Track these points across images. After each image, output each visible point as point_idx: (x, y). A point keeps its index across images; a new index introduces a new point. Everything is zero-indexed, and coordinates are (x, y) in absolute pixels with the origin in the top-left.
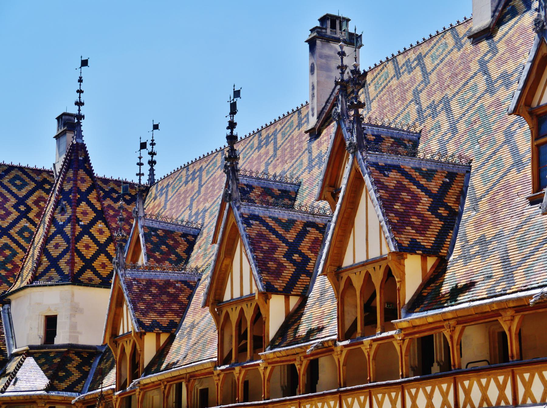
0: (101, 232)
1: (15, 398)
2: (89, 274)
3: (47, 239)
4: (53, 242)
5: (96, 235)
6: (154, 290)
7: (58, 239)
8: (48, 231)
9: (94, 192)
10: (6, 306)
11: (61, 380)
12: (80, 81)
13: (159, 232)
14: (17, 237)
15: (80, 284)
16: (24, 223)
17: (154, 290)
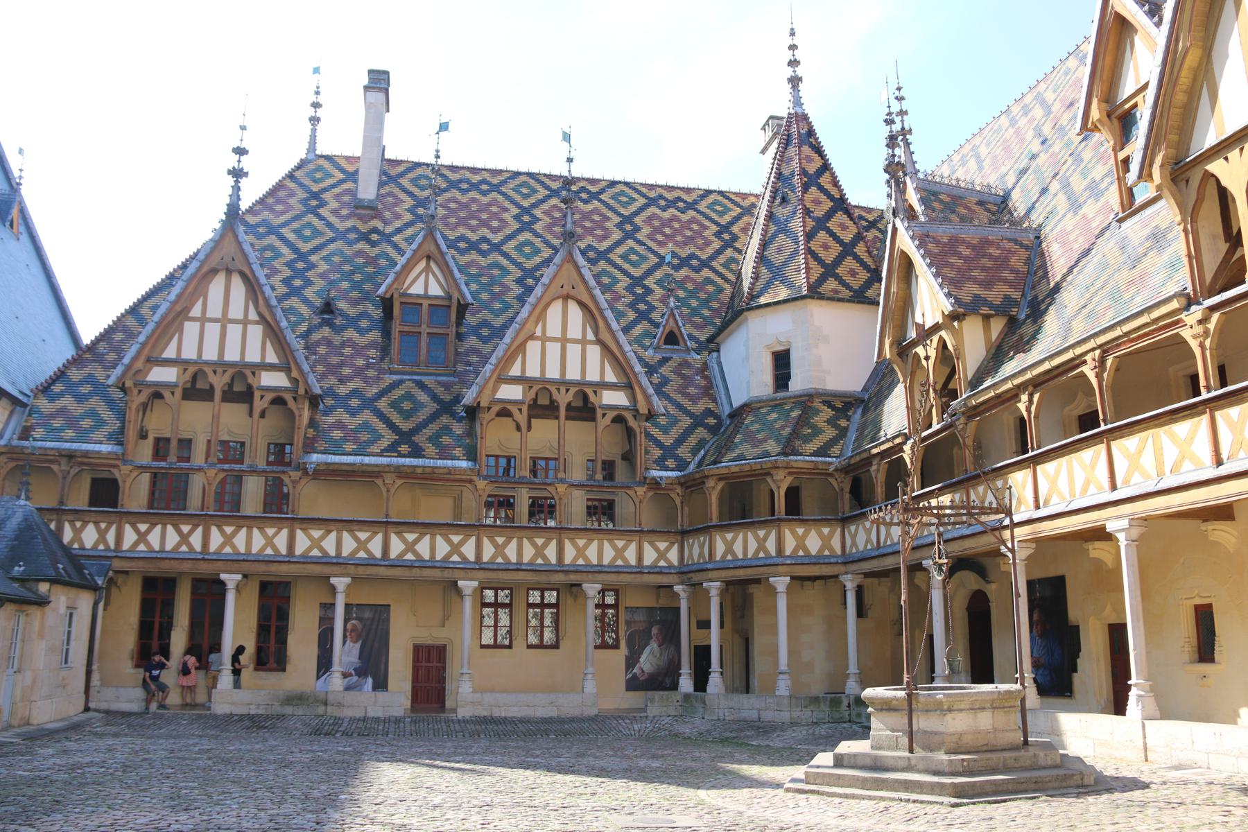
0: (843, 227)
1: (737, 469)
2: (831, 284)
3: (764, 245)
4: (774, 246)
5: (837, 231)
6: (966, 252)
7: (781, 240)
8: (765, 231)
9: (827, 174)
10: (715, 355)
11: (807, 439)
12: (792, 34)
13: (943, 197)
14: (721, 269)
15: (822, 297)
16: (729, 253)
17: (966, 252)
